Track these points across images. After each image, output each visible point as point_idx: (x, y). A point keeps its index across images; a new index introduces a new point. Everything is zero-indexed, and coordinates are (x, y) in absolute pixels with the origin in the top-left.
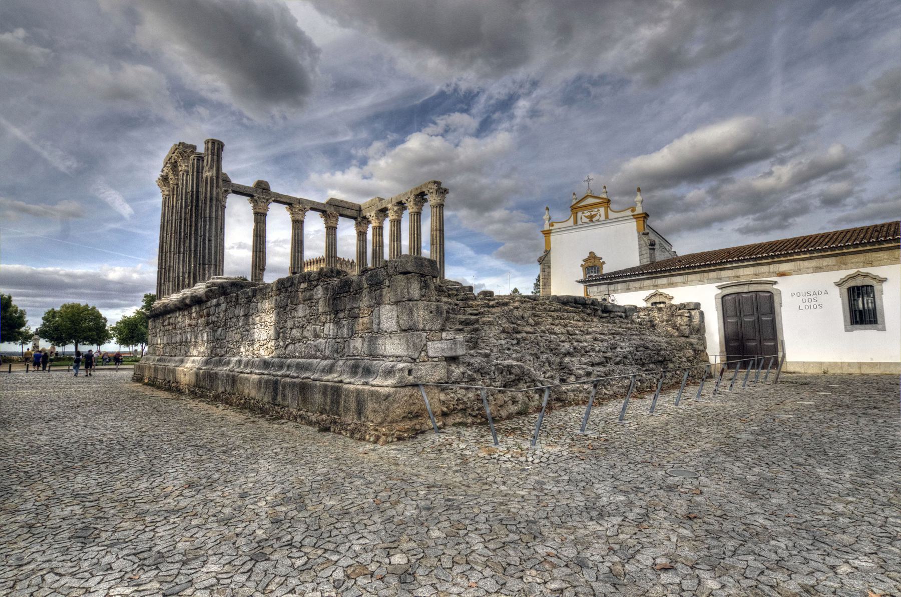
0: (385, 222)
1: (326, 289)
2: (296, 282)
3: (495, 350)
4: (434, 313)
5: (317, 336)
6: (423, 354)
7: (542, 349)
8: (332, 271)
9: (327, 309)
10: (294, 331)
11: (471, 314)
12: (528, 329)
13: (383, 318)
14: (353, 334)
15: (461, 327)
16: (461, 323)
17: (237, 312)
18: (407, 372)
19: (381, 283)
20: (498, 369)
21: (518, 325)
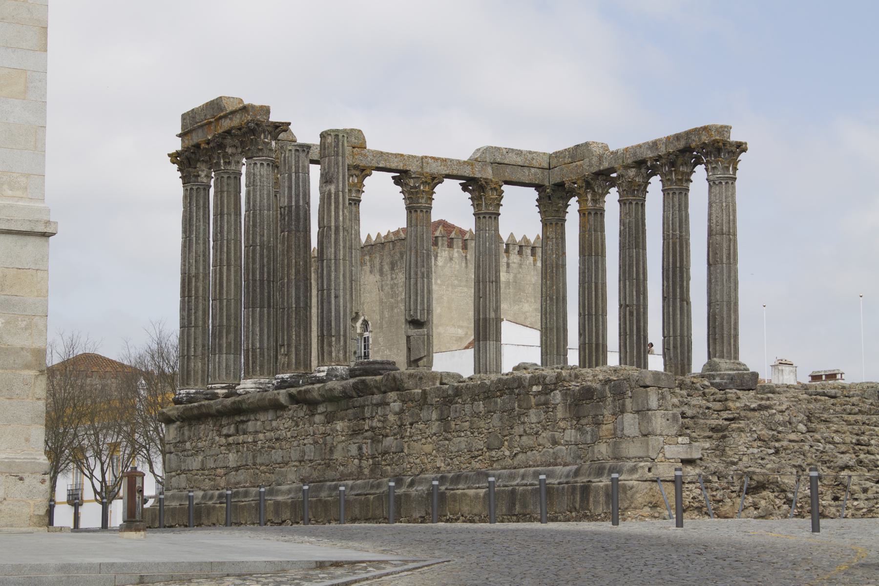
0: (607, 198)
1: (565, 395)
2: (526, 384)
3: (745, 459)
4: (671, 420)
5: (555, 443)
6: (661, 455)
8: (570, 376)
9: (568, 415)
10: (524, 438)
11: (726, 419)
12: (793, 436)
13: (626, 424)
14: (597, 439)
15: (711, 434)
16: (712, 429)
17: (424, 414)
18: (647, 469)
19: (624, 393)
20: (737, 474)
21: (779, 432)
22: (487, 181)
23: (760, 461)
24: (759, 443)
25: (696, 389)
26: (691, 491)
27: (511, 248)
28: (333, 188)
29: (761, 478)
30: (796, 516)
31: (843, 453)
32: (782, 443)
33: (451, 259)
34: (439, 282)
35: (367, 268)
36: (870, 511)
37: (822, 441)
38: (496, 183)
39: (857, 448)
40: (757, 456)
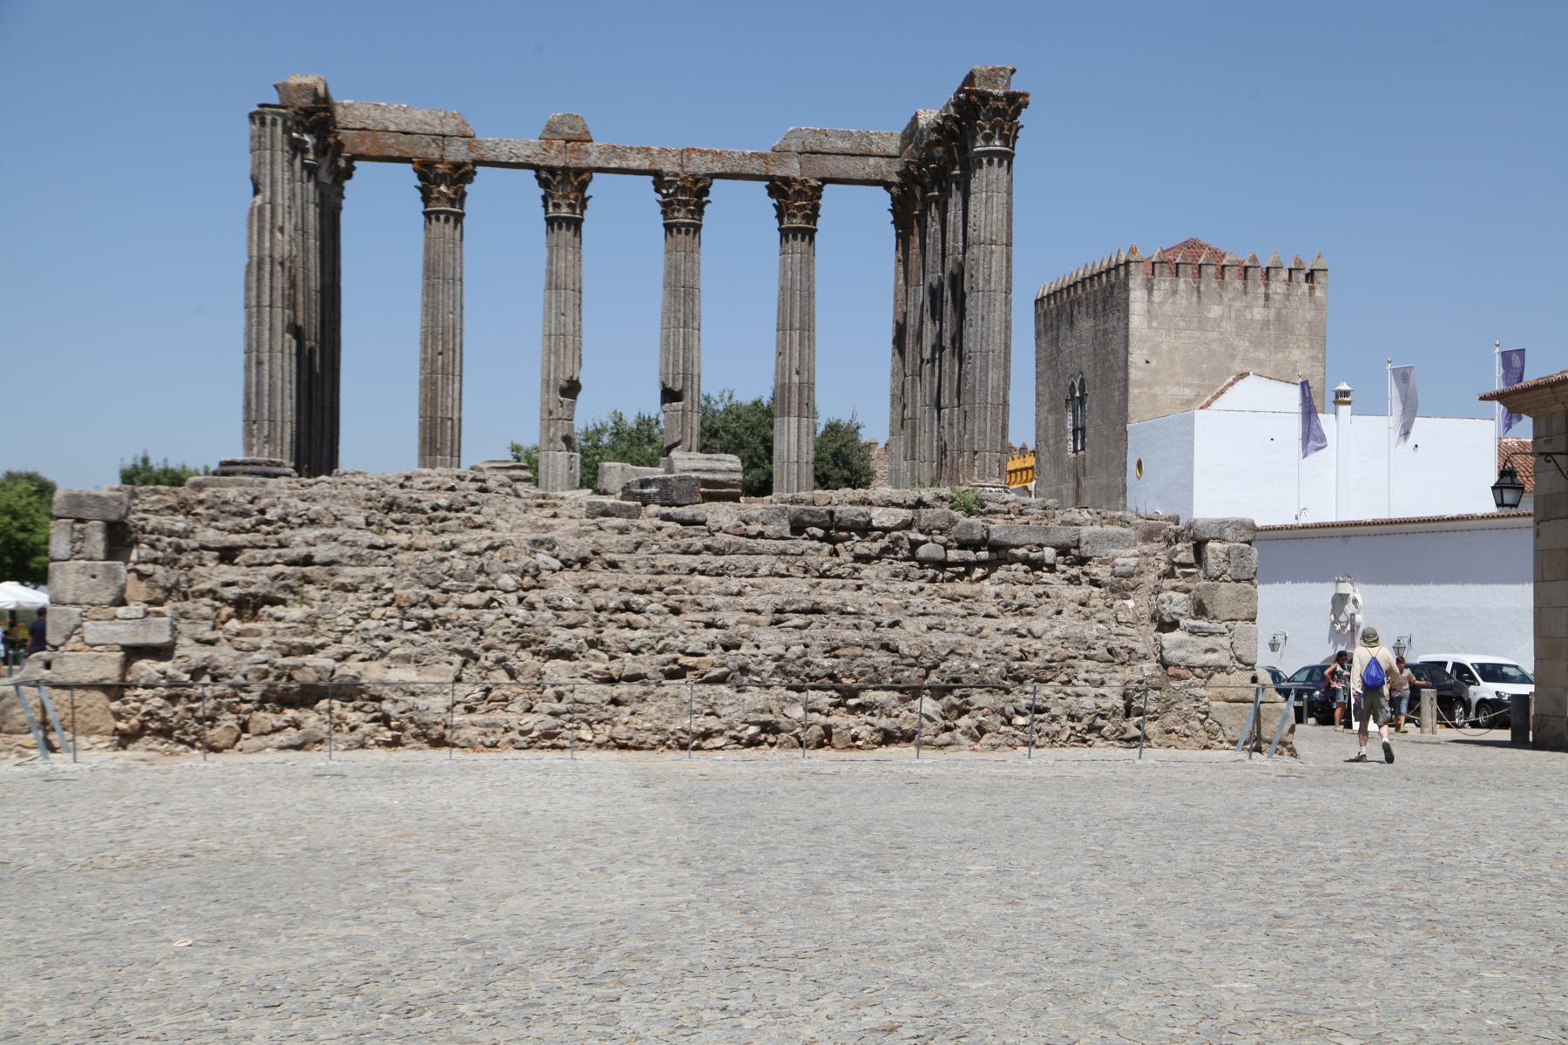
6: (74, 638)
7: (487, 641)
12: (473, 598)
18: (41, 664)
21: (446, 591)
22: (787, 181)
23: (381, 643)
24: (391, 611)
25: (423, 512)
26: (143, 701)
27: (1272, 272)
28: (259, 199)
29: (310, 677)
30: (388, 744)
31: (570, 627)
32: (440, 611)
33: (1175, 292)
34: (1155, 324)
35: (1083, 309)
36: (548, 735)
37: (540, 605)
38: (803, 183)
39: (603, 616)
40: (372, 634)
